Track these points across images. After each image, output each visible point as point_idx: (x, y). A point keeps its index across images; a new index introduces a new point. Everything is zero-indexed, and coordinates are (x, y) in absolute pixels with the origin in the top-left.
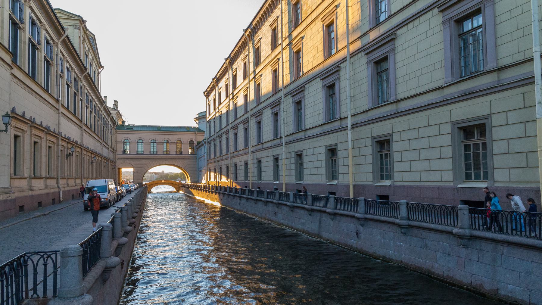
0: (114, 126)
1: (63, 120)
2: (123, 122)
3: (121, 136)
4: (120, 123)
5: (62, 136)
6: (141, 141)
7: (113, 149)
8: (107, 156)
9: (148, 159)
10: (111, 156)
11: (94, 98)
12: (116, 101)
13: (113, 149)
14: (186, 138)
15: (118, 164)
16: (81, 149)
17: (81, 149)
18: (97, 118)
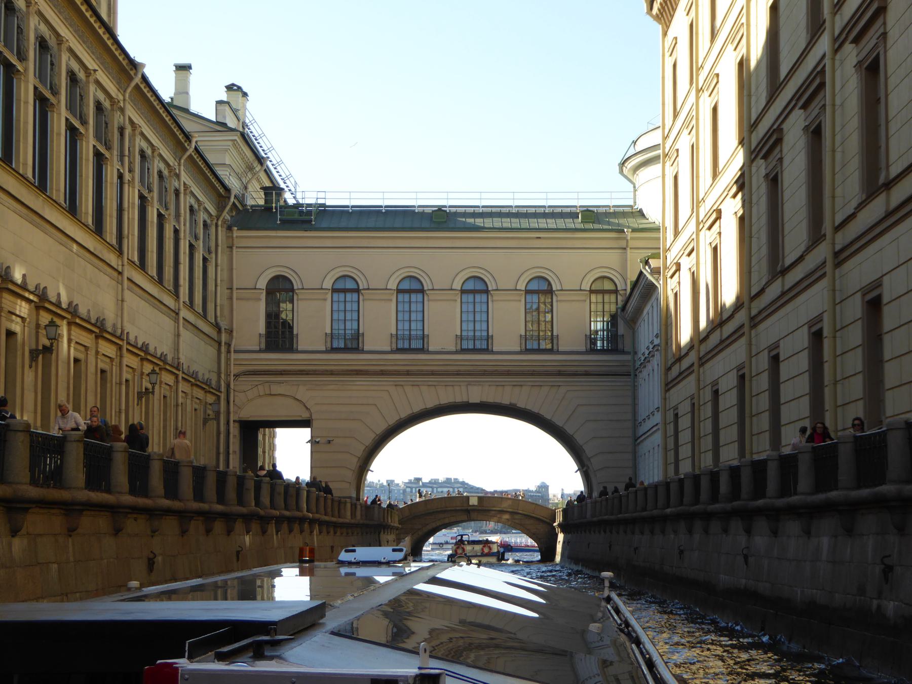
0: (220, 208)
2: (273, 190)
3: (260, 258)
4: (256, 198)
6: (350, 285)
7: (217, 327)
8: (161, 344)
9: (383, 373)
10: (196, 354)
11: (64, 31)
12: (230, 88)
13: (217, 327)
15: (237, 398)
16: (120, 348)
17: (120, 348)
18: (88, 145)
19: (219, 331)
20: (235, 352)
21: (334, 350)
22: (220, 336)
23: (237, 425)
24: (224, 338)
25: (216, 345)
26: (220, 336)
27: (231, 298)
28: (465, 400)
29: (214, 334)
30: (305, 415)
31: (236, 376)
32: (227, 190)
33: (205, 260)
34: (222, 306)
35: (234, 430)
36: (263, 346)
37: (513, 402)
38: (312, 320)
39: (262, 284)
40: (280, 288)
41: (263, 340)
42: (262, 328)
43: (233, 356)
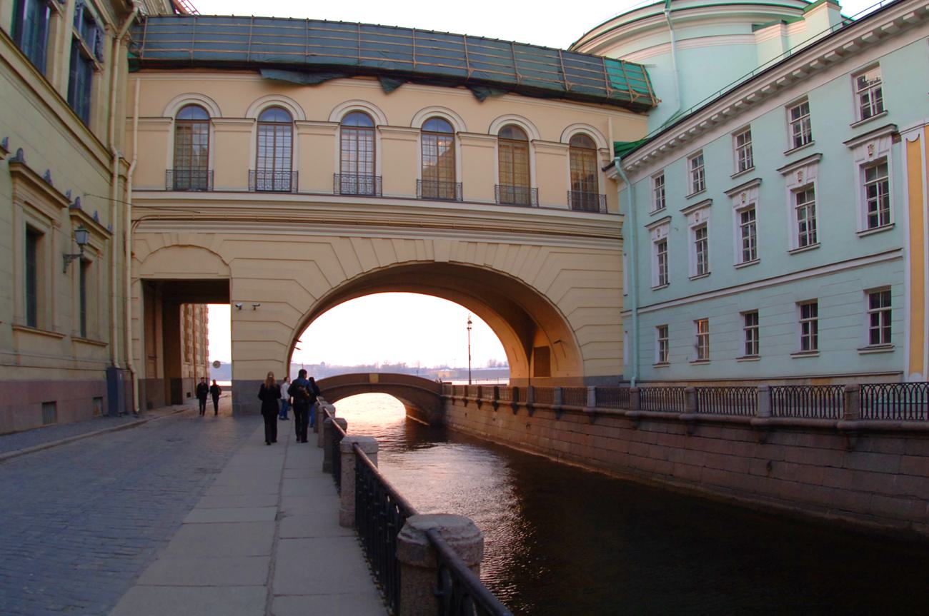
19: (112, 158)
20: (133, 191)
23: (138, 285)
24: (118, 168)
25: (108, 178)
28: (430, 258)
34: (117, 130)
35: (136, 292)
36: (171, 185)
37: (489, 263)
41: (171, 176)
42: (170, 166)
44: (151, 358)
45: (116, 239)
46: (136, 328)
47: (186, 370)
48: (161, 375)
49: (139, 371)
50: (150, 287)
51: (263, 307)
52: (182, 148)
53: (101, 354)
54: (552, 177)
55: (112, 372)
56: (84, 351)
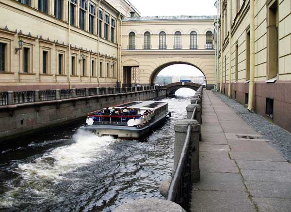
1: (73, 36)
5: (71, 47)
14: (202, 29)
19: (117, 45)
21: (144, 49)
22: (117, 46)
24: (119, 47)
26: (117, 46)
27: (121, 37)
29: (116, 46)
30: (137, 65)
31: (122, 56)
32: (119, 12)
33: (112, 29)
35: (122, 68)
38: (139, 43)
39: (128, 34)
40: (132, 34)
43: (121, 51)
44: (124, 79)
45: (119, 60)
46: (122, 75)
47: (133, 82)
48: (127, 83)
49: (122, 82)
50: (125, 67)
51: (145, 71)
52: (130, 42)
53: (116, 80)
54: (201, 42)
55: (117, 83)
56: (113, 79)
